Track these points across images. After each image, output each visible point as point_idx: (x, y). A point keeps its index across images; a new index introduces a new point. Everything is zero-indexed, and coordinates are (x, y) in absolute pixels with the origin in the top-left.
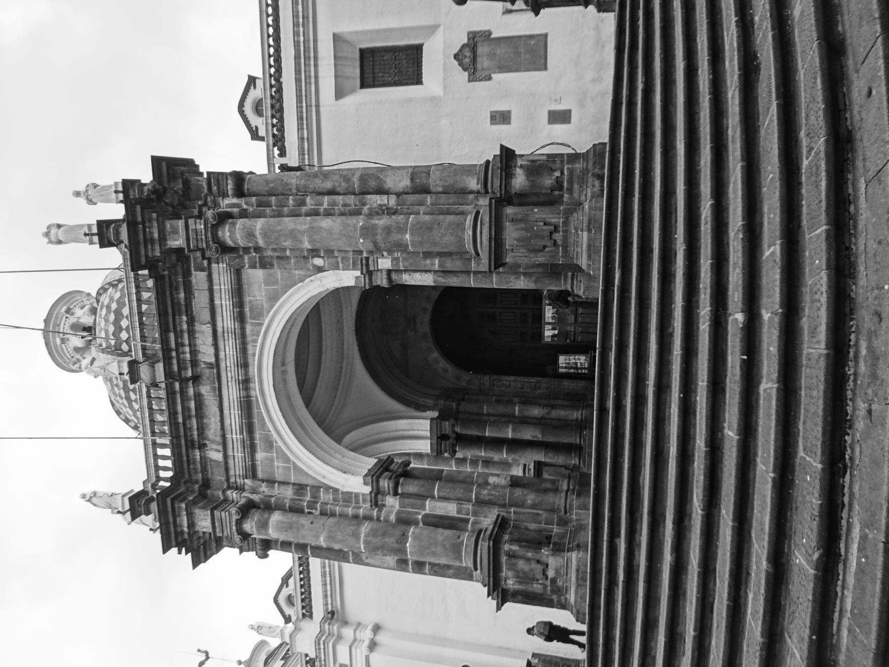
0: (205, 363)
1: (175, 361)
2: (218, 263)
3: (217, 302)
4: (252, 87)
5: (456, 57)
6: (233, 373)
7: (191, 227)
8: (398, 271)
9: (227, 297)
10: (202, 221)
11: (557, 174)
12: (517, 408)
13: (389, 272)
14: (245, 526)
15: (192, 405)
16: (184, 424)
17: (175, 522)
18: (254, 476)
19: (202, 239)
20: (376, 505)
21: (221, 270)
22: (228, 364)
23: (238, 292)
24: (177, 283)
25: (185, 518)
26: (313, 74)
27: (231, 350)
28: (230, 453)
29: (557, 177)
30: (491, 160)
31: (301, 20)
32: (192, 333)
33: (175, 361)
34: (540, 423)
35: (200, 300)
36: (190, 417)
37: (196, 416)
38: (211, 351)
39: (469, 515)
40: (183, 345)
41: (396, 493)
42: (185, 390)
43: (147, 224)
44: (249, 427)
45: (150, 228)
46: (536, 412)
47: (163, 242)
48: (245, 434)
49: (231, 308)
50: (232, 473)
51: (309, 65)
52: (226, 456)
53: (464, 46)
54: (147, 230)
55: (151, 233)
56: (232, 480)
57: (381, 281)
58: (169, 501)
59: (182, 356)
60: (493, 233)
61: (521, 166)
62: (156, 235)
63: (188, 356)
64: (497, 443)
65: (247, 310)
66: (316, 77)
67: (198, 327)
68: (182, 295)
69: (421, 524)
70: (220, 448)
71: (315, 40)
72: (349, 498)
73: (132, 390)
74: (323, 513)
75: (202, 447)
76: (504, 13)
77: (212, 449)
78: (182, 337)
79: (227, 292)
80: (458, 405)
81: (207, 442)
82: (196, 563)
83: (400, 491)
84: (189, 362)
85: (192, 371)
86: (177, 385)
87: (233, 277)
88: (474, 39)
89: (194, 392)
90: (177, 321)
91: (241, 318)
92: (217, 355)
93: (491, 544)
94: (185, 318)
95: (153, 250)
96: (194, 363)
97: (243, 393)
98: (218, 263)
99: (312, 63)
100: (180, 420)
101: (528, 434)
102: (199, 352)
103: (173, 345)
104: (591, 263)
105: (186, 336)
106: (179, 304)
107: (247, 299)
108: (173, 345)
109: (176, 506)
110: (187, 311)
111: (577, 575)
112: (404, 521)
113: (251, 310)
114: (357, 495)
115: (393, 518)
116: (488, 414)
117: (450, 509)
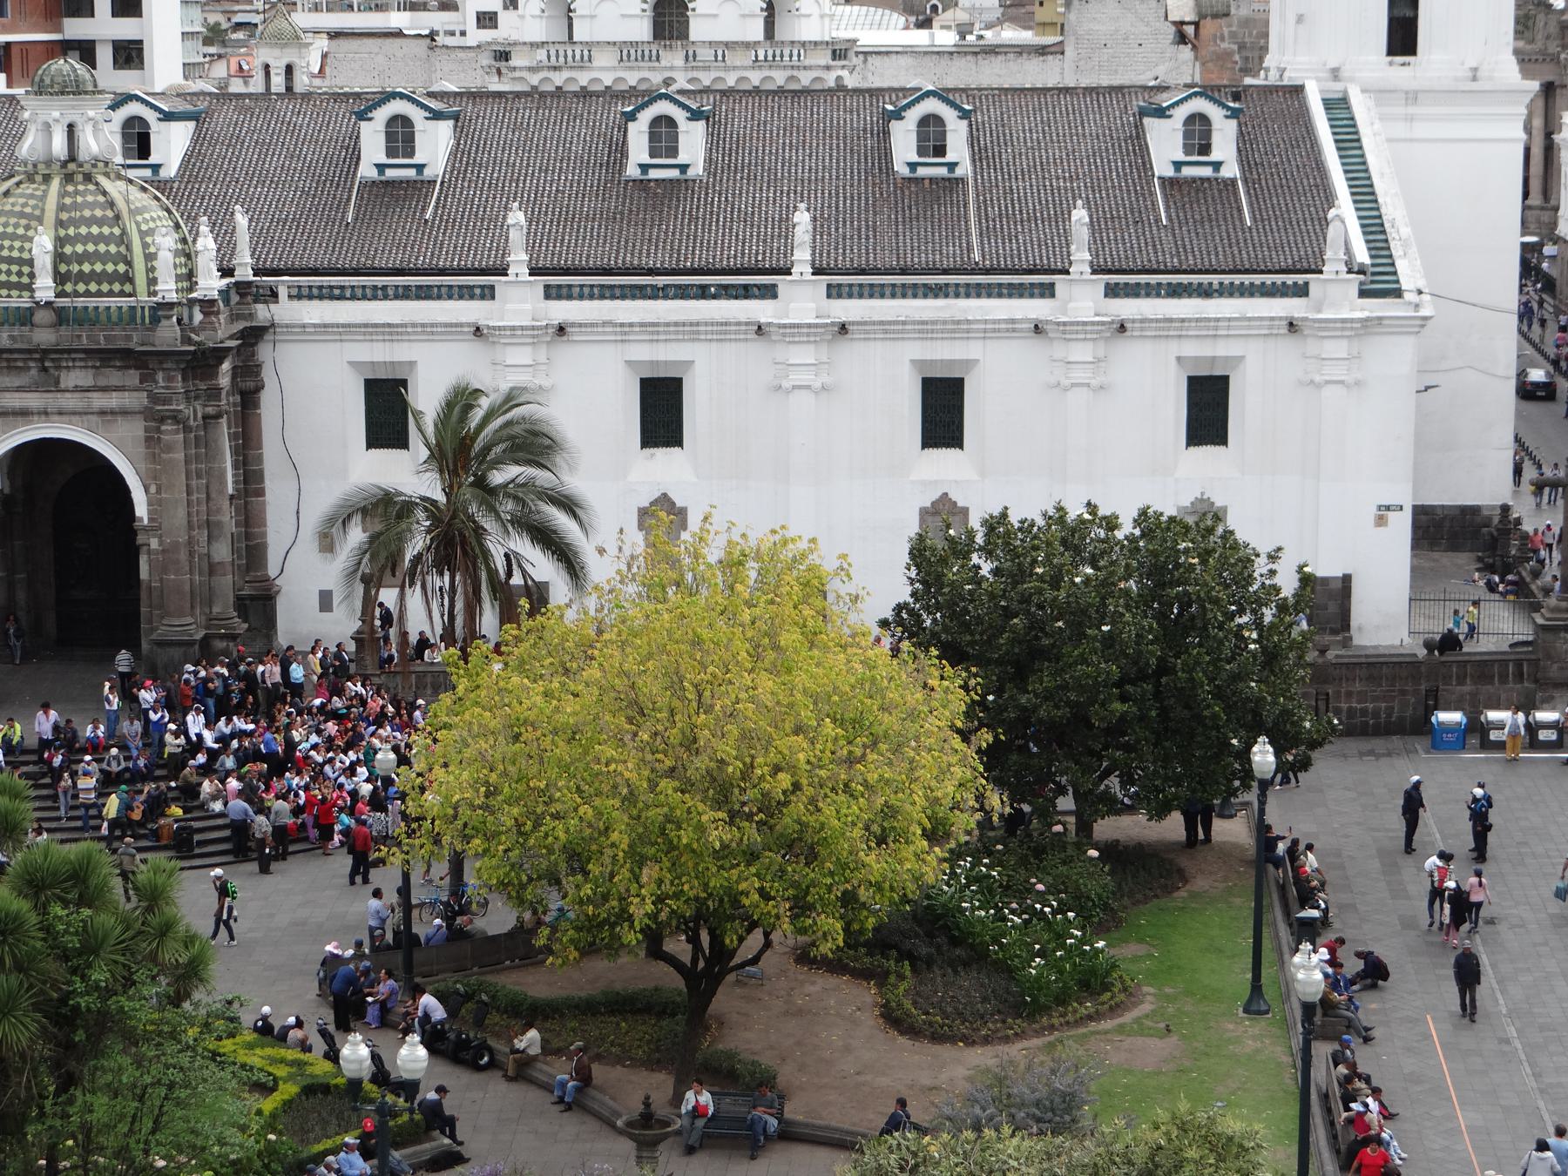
0: (59, 376)
3: (114, 394)
4: (427, 115)
15: (20, 364)
23: (125, 412)
35: (114, 377)
38: (71, 384)
46: (21, 596)
57: (141, 539)
65: (109, 418)
86: (37, 356)
91: (102, 413)
96: (58, 368)
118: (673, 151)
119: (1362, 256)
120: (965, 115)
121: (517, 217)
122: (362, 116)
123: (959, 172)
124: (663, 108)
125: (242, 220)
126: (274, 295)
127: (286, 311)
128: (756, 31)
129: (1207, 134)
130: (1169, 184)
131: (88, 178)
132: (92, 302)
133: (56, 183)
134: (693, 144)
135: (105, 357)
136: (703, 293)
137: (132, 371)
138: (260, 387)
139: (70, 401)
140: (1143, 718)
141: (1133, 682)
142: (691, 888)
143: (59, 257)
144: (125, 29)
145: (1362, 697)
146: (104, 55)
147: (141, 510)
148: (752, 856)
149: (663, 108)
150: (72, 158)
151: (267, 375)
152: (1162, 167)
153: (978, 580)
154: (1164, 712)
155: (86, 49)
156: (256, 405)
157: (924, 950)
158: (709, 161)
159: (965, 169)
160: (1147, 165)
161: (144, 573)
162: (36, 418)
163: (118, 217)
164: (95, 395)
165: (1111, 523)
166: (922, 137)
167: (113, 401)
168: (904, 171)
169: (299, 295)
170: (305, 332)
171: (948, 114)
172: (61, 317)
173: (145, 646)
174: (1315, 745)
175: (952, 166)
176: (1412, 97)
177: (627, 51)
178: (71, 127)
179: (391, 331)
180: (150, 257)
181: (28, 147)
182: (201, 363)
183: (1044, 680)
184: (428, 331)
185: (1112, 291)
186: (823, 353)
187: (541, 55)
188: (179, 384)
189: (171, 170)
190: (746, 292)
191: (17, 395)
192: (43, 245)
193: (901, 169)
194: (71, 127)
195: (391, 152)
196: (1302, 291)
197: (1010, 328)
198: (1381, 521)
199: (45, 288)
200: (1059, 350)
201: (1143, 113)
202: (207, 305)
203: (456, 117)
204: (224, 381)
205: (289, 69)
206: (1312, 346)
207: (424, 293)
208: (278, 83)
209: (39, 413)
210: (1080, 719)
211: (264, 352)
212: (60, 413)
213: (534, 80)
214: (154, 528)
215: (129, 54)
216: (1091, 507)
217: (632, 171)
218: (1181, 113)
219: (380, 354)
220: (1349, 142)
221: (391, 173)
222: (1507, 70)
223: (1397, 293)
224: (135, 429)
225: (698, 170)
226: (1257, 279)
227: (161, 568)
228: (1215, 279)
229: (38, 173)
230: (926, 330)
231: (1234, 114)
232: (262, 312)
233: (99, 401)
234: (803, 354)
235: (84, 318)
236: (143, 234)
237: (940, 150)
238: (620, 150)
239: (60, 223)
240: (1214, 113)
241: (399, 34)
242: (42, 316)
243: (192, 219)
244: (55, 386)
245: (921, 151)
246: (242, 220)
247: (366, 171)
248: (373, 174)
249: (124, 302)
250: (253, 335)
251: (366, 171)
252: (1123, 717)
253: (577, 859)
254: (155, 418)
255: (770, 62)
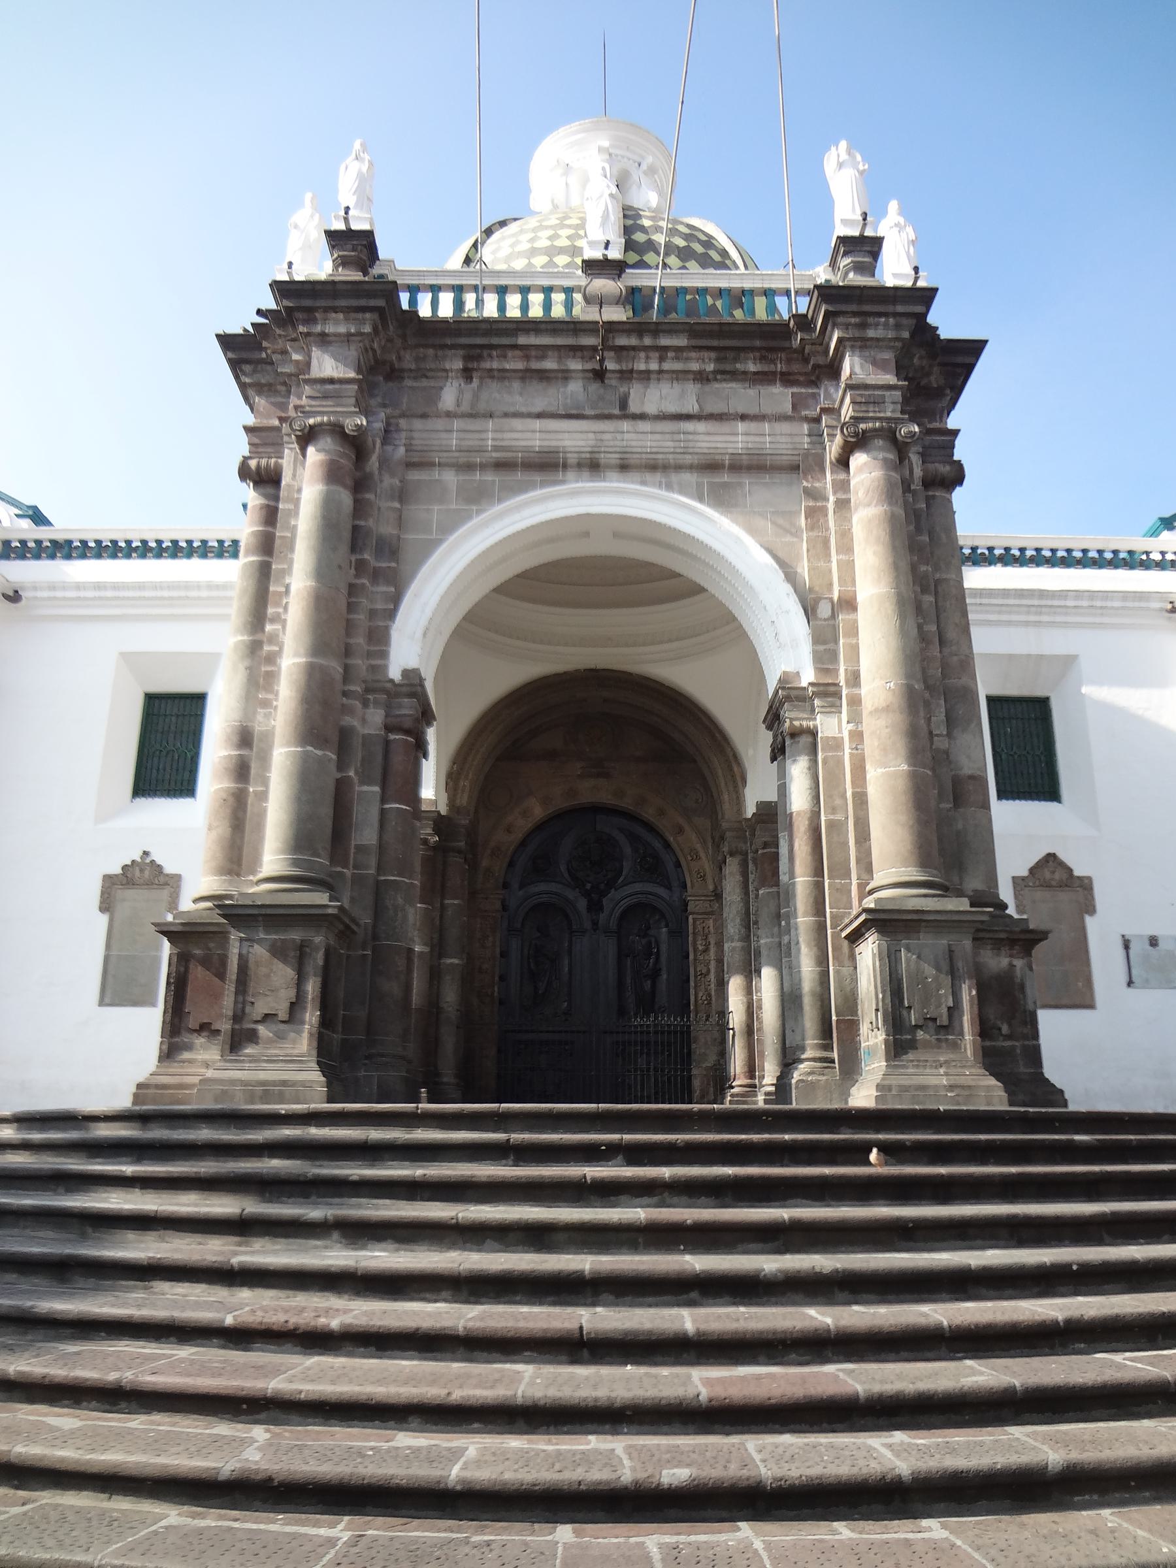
1: (633, 341)
2: (809, 435)
3: (741, 426)
5: (1051, 858)
6: (612, 443)
7: (887, 393)
8: (813, 750)
9: (750, 446)
10: (899, 415)
11: (1005, 1029)
12: (456, 961)
13: (813, 733)
14: (329, 440)
15: (550, 364)
16: (515, 347)
17: (335, 310)
18: (410, 465)
19: (867, 411)
20: (368, 690)
21: (797, 439)
22: (626, 436)
24: (773, 361)
25: (342, 329)
26: (1014, 618)
27: (654, 444)
28: (456, 424)
29: (1000, 1029)
30: (1007, 912)
31: (1098, 604)
32: (678, 376)
33: (633, 341)
35: (740, 396)
36: (527, 358)
37: (527, 370)
38: (651, 408)
39: (355, 867)
40: (662, 359)
41: (389, 728)
42: (579, 354)
43: (891, 320)
45: (886, 325)
47: (859, 343)
48: (494, 455)
49: (730, 451)
50: (418, 424)
51: (1028, 613)
52: (449, 415)
53: (1070, 870)
54: (883, 320)
55: (877, 325)
56: (403, 423)
58: (380, 303)
59: (642, 355)
60: (931, 917)
61: (1012, 966)
62: (871, 333)
63: (642, 366)
65: (726, 478)
66: (1009, 623)
67: (692, 389)
68: (752, 367)
69: (339, 776)
70: (465, 407)
71: (1066, 625)
72: (379, 639)
73: (551, 260)
74: (352, 589)
75: (467, 374)
76: (1123, 936)
77: (461, 391)
78: (677, 358)
79: (759, 446)
80: (460, 852)
81: (476, 382)
82: (226, 341)
83: (392, 737)
84: (630, 367)
85: (613, 371)
87: (785, 458)
88: (1081, 886)
89: (574, 371)
90: (706, 354)
91: (711, 466)
92: (642, 417)
93: (330, 911)
94: (711, 367)
95: (847, 326)
96: (627, 375)
97: (572, 459)
98: (809, 435)
99: (1032, 618)
100: (522, 340)
102: (647, 387)
103: (665, 341)
104: (894, 1092)
105: (678, 366)
106: (736, 360)
107: (746, 480)
108: (665, 341)
109: (368, 315)
110: (723, 372)
111: (274, 1083)
113: (725, 485)
114: (384, 655)
115: (348, 721)
116: (443, 907)
137: (777, 390)
162: (570, 475)
164: (701, 427)
191: (537, 424)
209: (580, 466)
212: (624, 467)
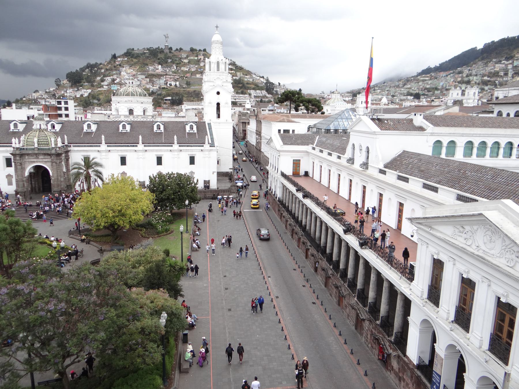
23: (48, 162)
34: (35, 186)
35: (46, 157)
44: (31, 162)
46: (37, 186)
64: (31, 181)
72: (25, 174)
101: (33, 185)
112: (23, 181)
117: (26, 185)
118: (125, 129)
119: (210, 142)
120: (163, 124)
121: (103, 137)
122: (84, 124)
123: (162, 131)
124: (124, 123)
125: (66, 137)
126: (71, 146)
127: (72, 148)
128: (142, 114)
129: (193, 127)
130: (188, 133)
131: (43, 131)
132: (43, 147)
133: (38, 132)
134: (128, 128)
135: (45, 154)
136: (128, 146)
138: (69, 158)
139: (41, 160)
140: (177, 198)
141: (176, 193)
142: (109, 221)
143: (38, 141)
144: (67, 112)
145: (210, 194)
146: (64, 116)
147: (51, 174)
148: (117, 216)
149: (124, 123)
150: (40, 128)
151: (70, 156)
152: (187, 131)
153: (156, 181)
154: (179, 197)
155: (60, 116)
156: (69, 160)
157: (147, 227)
158: (130, 130)
159: (163, 131)
160: (185, 131)
161: (52, 182)
163: (47, 136)
165: (174, 174)
166: (157, 127)
167: (46, 160)
168: (155, 131)
169: (74, 146)
170: (75, 151)
171: (161, 124)
172: (39, 149)
173: (52, 192)
174: (200, 200)
175: (161, 131)
176: (219, 123)
177: (125, 116)
178: (40, 125)
179: (87, 151)
180: (51, 142)
181: (34, 127)
182: (58, 155)
183: (164, 193)
184: (91, 151)
185: (180, 146)
186: (144, 153)
187: (114, 116)
188: (55, 158)
189: (58, 130)
190: (134, 146)
192: (36, 140)
193: (155, 131)
194: (40, 125)
195: (88, 128)
196: (203, 146)
197: (167, 151)
198: (213, 174)
199: (36, 145)
200: (173, 153)
201: (186, 124)
202: (59, 148)
203: (97, 124)
204: (63, 158)
205: (81, 118)
206: (204, 153)
207: (91, 146)
208: (80, 119)
210: (168, 199)
211: (69, 154)
213: (113, 119)
214: (53, 176)
215: (67, 116)
216: (172, 172)
217: (120, 131)
218: (189, 125)
219: (86, 154)
220: (210, 128)
221: (88, 131)
222: (230, 120)
223: (214, 146)
224: (50, 164)
225: (129, 131)
226: (197, 145)
227: (54, 181)
228: (192, 145)
229: (36, 131)
230: (157, 151)
231: (196, 125)
232: (69, 149)
233: (44, 160)
234: (141, 154)
235: (42, 149)
236: (50, 139)
237: (160, 129)
238: (118, 128)
239: (38, 137)
240: (193, 125)
241: (102, 114)
242: (36, 149)
243: (58, 137)
244: (38, 158)
245: (157, 129)
246: (66, 137)
247: (85, 131)
248: (86, 131)
249: (48, 147)
250: (67, 152)
251: (85, 131)
252: (174, 198)
253: (95, 217)
254: (52, 162)
255: (144, 118)
